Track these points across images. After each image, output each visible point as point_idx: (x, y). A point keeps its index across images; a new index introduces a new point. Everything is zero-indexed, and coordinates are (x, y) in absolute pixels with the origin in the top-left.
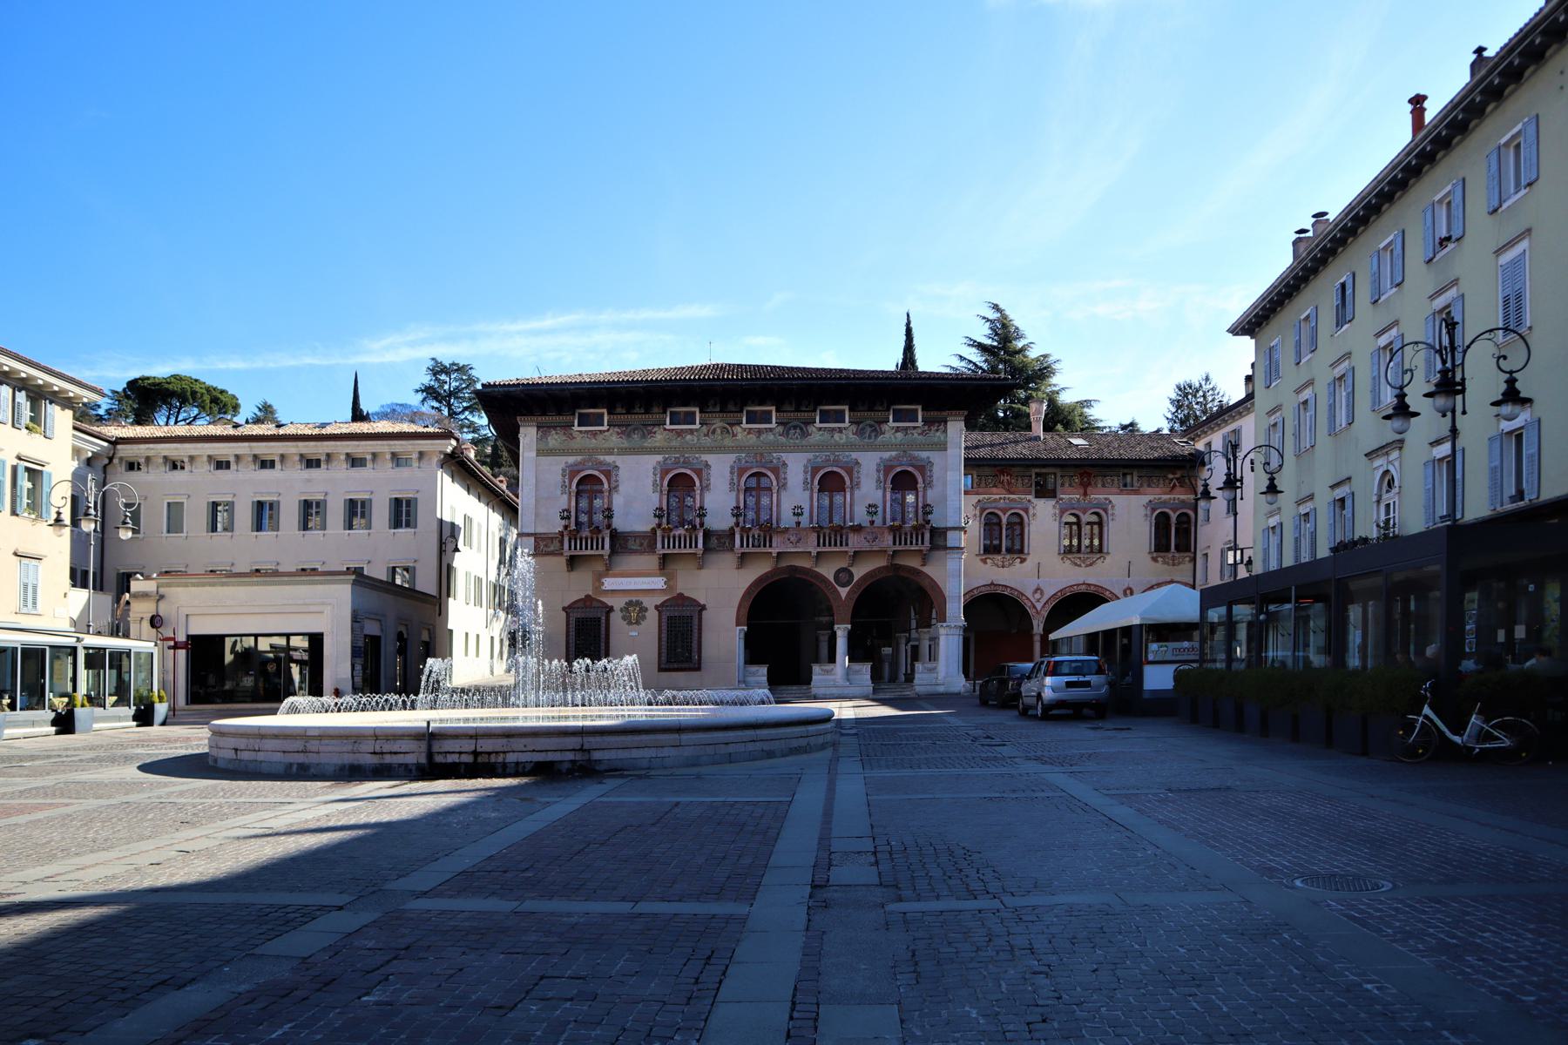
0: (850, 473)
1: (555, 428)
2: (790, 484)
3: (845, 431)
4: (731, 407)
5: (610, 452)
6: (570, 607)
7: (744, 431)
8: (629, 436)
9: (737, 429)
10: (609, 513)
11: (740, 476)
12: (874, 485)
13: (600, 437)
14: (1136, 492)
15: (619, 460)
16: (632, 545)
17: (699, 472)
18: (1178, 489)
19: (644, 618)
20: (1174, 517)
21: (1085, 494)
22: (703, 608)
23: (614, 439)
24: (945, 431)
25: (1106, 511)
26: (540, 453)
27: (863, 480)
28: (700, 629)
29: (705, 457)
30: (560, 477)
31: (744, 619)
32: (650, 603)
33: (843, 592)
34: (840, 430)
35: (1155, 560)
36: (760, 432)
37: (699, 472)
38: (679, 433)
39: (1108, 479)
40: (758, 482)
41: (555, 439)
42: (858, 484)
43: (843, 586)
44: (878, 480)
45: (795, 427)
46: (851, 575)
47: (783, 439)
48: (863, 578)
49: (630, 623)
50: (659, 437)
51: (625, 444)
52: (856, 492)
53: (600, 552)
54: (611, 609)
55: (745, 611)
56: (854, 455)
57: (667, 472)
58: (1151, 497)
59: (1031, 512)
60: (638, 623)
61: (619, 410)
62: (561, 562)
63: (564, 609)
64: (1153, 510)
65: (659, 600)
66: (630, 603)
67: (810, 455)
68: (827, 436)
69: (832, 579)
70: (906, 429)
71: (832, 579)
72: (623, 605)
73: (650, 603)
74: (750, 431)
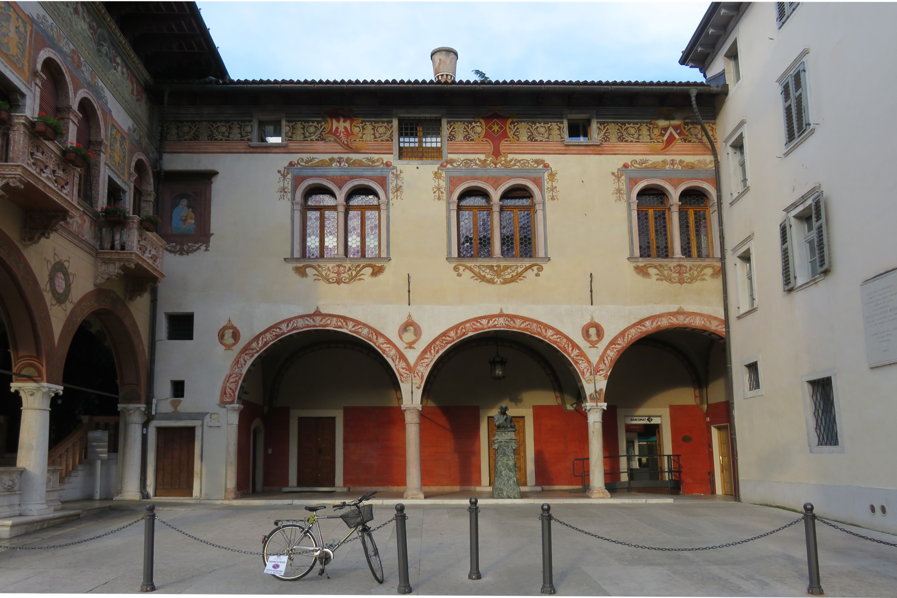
14: (597, 149)
18: (679, 144)
20: (674, 194)
21: (497, 153)
25: (538, 182)
35: (642, 271)
39: (541, 128)
58: (627, 159)
59: (392, 184)
64: (633, 182)
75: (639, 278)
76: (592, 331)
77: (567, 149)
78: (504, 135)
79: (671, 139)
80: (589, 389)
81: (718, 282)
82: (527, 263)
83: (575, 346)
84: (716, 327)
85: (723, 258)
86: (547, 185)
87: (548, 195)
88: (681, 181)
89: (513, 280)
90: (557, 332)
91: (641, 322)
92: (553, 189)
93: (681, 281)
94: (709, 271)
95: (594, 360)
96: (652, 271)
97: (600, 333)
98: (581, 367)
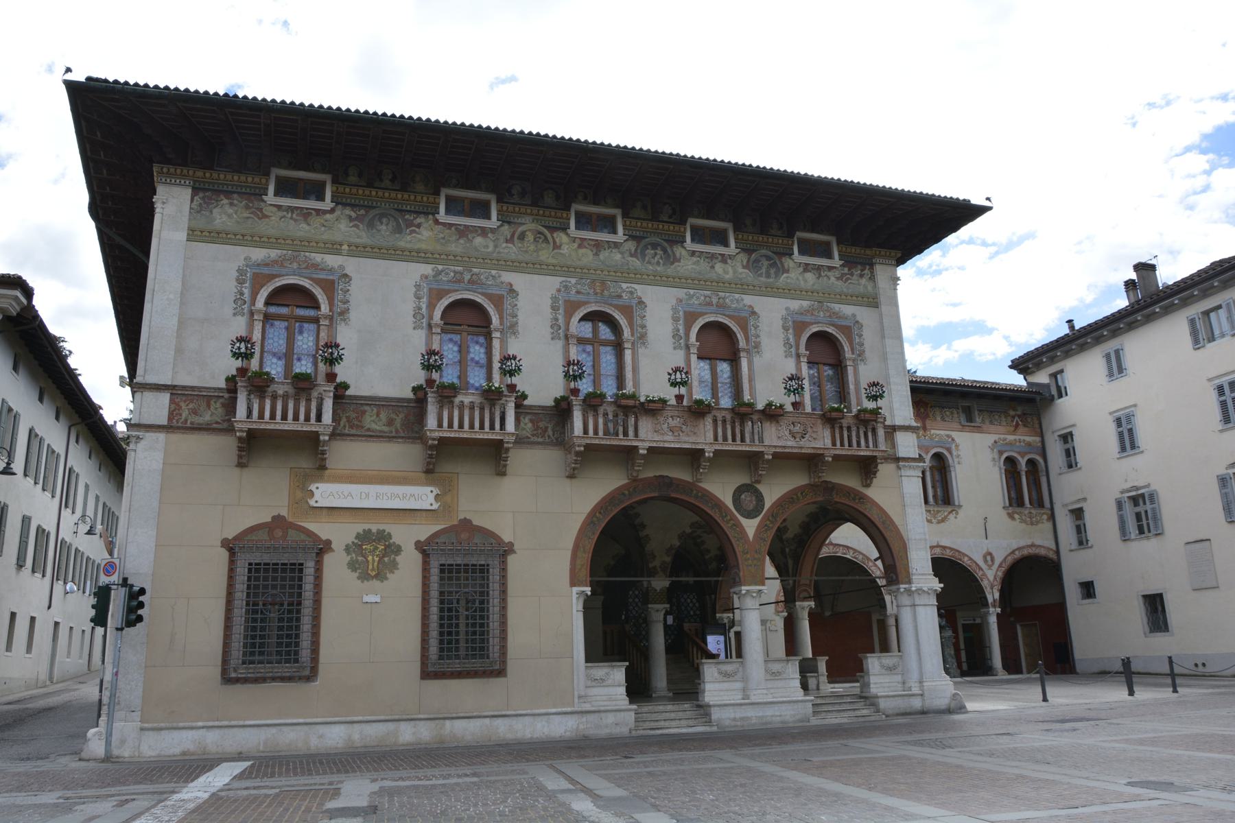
0: (745, 328)
1: (228, 194)
2: (651, 336)
3: (731, 262)
4: (549, 199)
5: (334, 248)
6: (236, 538)
7: (572, 243)
8: (371, 225)
9: (561, 237)
10: (331, 355)
11: (569, 316)
12: (781, 350)
13: (316, 221)
14: (979, 429)
15: (352, 265)
16: (372, 421)
17: (498, 301)
18: (1022, 429)
19: (394, 566)
20: (1023, 462)
22: (508, 549)
23: (343, 227)
24: (872, 278)
26: (195, 235)
27: (765, 341)
28: (504, 592)
29: (507, 277)
30: (232, 286)
31: (584, 573)
32: (407, 536)
33: (750, 526)
34: (724, 259)
35: (1011, 516)
36: (598, 246)
37: (498, 301)
38: (463, 232)
40: (595, 331)
41: (225, 215)
42: (757, 345)
43: (750, 515)
44: (787, 343)
45: (654, 246)
46: (760, 498)
47: (636, 263)
48: (780, 504)
49: (365, 577)
50: (425, 235)
51: (362, 236)
52: (757, 360)
53: (312, 427)
54: (322, 549)
55: (585, 558)
56: (748, 300)
57: (441, 294)
58: (996, 437)
60: (380, 576)
61: (353, 179)
62: (227, 445)
63: (226, 544)
64: (1001, 453)
65: (424, 531)
66: (365, 537)
67: (681, 293)
68: (704, 265)
69: (729, 502)
70: (819, 268)
71: (729, 502)
72: (350, 538)
73: (407, 536)
74: (582, 243)
75: (1009, 520)
76: (989, 556)
77: (963, 428)
78: (927, 416)
79: (1017, 426)
80: (990, 600)
81: (1049, 525)
82: (949, 509)
83: (981, 569)
84: (1052, 555)
85: (1052, 509)
86: (955, 453)
87: (956, 460)
88: (1026, 453)
89: (943, 521)
90: (971, 559)
91: (1013, 552)
92: (958, 456)
93: (1032, 524)
94: (1045, 517)
95: (991, 578)
96: (1016, 516)
97: (993, 560)
98: (985, 583)
